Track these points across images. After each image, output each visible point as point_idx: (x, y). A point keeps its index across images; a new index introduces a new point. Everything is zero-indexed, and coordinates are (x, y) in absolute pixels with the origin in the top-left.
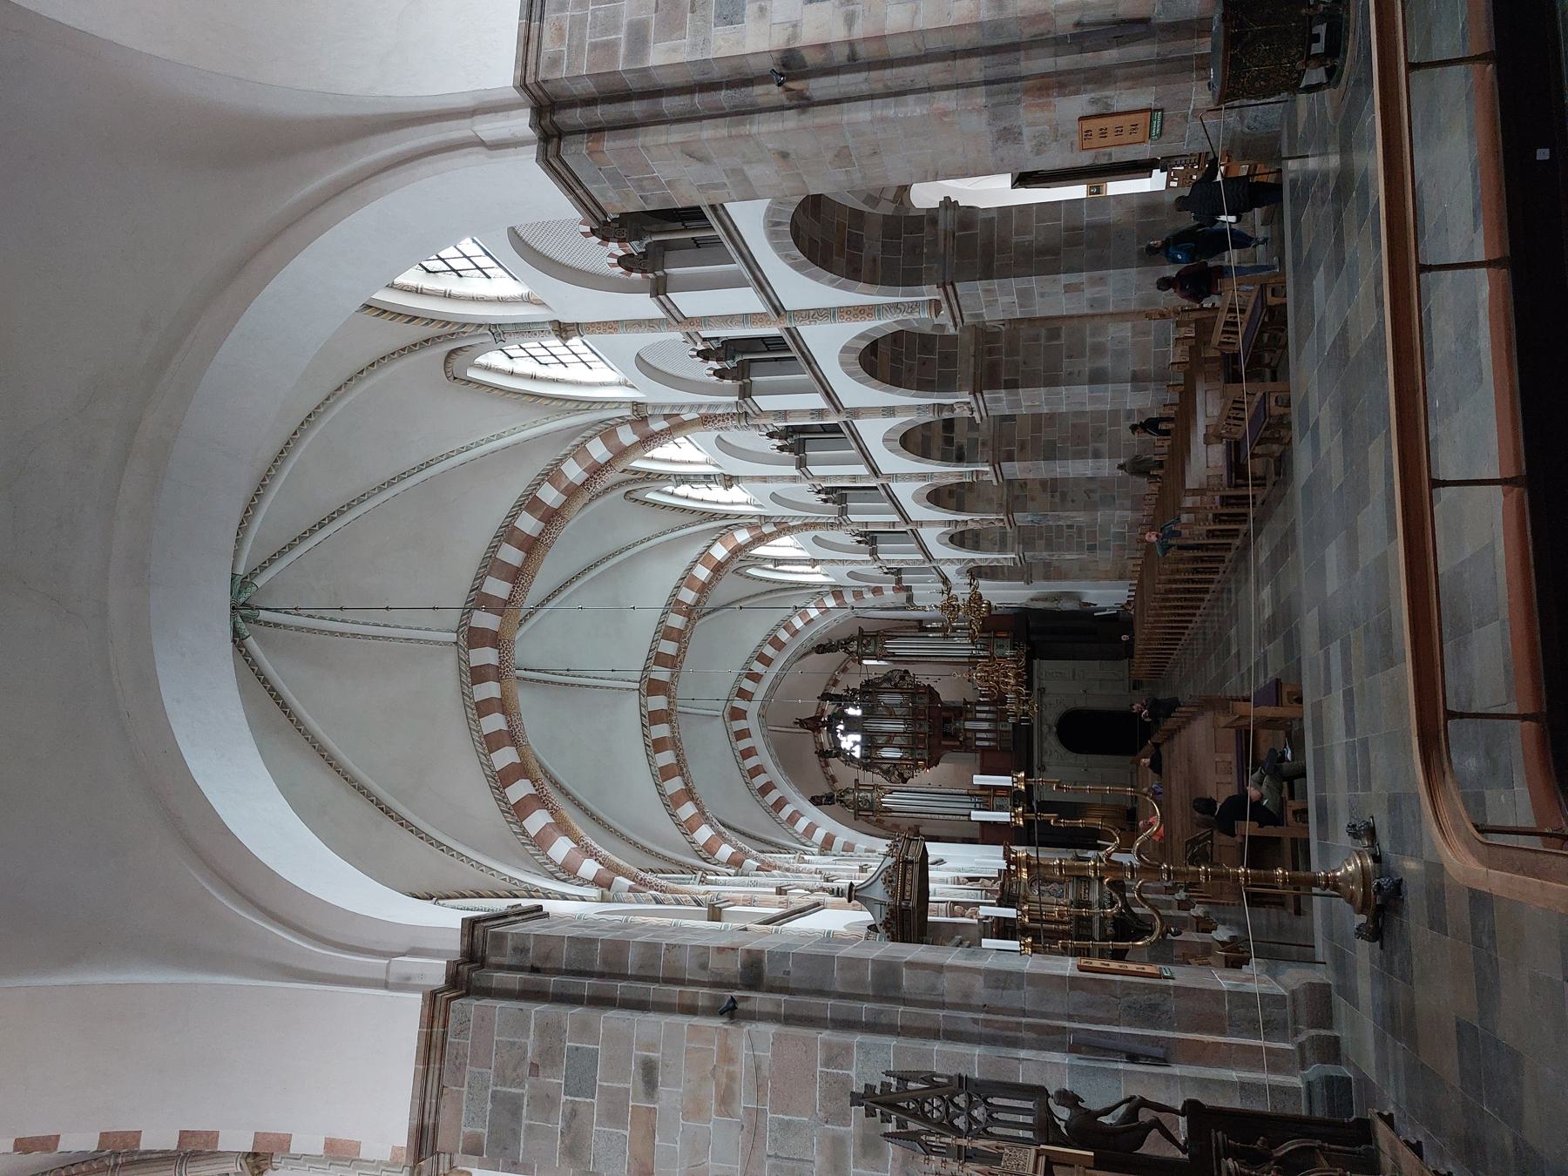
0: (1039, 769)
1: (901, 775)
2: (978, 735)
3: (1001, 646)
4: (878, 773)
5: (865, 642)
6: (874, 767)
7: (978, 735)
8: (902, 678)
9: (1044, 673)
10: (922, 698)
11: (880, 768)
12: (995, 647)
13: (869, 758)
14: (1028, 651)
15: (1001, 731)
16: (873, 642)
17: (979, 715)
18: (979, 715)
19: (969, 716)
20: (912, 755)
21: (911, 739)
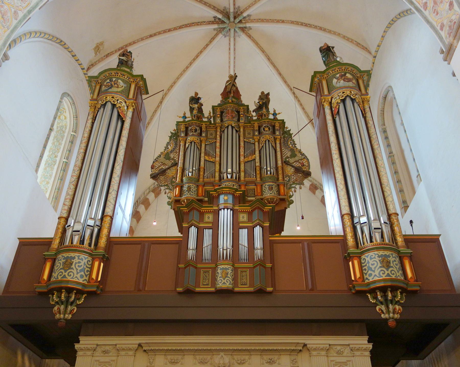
0: (140, 345)
1: (163, 172)
2: (208, 234)
3: (386, 264)
4: (166, 148)
5: (348, 75)
6: (176, 144)
7: (208, 234)
8: (297, 170)
9: (344, 359)
10: (271, 188)
11: (171, 152)
12: (381, 253)
13: (187, 134)
14: (386, 320)
15: (214, 270)
16: (350, 84)
17: (244, 233)
18: (244, 233)
19: (243, 217)
20: (190, 180)
21: (212, 180)
